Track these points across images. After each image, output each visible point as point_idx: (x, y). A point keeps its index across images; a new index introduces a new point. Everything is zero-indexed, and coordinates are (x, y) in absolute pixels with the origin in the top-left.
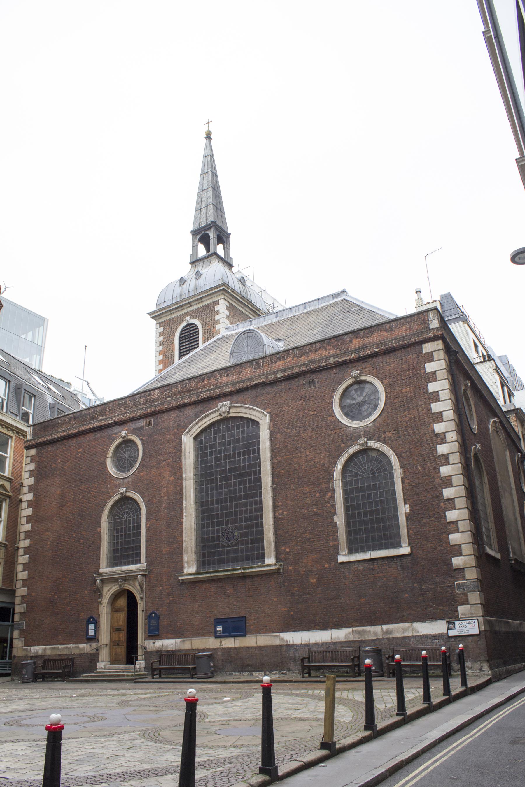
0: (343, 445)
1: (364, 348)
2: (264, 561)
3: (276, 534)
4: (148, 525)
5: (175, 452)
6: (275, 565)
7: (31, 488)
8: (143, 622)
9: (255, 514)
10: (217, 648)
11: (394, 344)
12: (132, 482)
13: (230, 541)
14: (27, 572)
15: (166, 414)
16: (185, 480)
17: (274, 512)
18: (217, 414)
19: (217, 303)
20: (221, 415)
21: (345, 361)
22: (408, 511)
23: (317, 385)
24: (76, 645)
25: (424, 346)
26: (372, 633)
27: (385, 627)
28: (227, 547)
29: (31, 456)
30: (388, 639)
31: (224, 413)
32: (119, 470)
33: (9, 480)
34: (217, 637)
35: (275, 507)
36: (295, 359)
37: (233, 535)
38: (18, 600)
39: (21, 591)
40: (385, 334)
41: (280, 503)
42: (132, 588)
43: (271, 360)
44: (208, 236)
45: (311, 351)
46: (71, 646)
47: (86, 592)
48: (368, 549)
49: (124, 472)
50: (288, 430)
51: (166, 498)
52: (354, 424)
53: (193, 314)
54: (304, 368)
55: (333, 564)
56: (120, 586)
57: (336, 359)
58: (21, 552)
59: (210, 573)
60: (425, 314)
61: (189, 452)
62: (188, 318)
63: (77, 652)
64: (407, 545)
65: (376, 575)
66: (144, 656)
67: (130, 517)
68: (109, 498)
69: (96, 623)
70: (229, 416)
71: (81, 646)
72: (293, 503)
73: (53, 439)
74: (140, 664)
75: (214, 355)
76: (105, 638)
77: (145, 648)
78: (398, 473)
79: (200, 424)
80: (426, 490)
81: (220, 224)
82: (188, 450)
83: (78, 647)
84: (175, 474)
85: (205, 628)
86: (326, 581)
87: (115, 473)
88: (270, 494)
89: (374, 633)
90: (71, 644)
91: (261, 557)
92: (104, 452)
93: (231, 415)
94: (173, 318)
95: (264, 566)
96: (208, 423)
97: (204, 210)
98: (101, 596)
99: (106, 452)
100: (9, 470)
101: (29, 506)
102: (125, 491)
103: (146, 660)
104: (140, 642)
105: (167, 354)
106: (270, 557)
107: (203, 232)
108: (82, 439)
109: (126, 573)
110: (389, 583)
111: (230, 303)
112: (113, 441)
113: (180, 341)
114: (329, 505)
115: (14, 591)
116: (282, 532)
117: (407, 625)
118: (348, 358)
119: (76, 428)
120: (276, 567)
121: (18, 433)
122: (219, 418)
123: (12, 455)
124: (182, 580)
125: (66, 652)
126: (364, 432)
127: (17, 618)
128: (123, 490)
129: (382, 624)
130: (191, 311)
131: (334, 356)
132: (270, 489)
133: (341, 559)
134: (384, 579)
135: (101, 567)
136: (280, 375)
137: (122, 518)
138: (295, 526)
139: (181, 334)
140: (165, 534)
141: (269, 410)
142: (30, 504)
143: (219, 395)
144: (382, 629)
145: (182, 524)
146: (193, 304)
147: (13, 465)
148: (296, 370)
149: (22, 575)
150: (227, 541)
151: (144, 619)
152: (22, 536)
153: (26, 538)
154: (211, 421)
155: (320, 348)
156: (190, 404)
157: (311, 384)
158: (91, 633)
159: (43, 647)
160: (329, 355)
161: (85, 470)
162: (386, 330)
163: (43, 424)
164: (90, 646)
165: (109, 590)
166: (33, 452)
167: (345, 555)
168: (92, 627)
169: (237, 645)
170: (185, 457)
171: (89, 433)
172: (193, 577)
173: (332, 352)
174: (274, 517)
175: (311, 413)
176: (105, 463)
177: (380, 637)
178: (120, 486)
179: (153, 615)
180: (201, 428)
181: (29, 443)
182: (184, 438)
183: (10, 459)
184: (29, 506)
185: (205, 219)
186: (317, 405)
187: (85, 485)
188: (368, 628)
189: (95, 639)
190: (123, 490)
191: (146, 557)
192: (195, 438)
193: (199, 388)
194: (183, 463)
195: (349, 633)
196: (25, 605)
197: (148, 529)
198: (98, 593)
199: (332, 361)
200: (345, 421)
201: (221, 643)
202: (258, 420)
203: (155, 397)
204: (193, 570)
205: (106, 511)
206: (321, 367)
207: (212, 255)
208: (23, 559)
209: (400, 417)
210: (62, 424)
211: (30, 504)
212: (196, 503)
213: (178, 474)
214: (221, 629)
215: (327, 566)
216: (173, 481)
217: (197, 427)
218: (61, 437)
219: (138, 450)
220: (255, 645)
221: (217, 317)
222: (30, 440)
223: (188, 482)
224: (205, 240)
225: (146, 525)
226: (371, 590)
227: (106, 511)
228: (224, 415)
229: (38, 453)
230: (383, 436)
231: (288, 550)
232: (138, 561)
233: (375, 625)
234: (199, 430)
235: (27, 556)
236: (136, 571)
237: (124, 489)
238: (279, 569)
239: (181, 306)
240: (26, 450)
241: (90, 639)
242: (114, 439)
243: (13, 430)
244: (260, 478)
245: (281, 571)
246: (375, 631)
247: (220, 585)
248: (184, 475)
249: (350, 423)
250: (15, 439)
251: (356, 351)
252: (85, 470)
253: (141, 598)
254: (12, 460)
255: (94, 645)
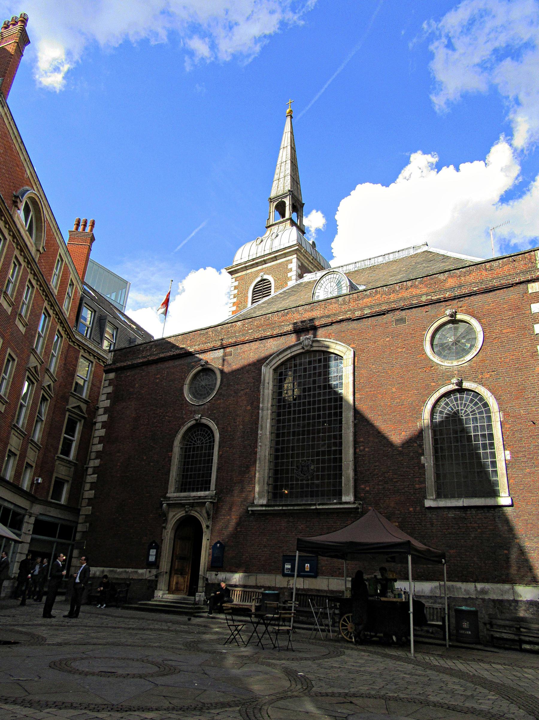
0: (433, 384)
1: (460, 287)
2: (341, 498)
3: (355, 471)
4: (221, 453)
5: (254, 383)
6: (354, 503)
7: (107, 410)
8: (207, 551)
9: (333, 448)
10: (284, 588)
11: (496, 283)
12: (208, 409)
13: (305, 475)
14: (94, 491)
15: (247, 345)
16: (262, 410)
17: (355, 448)
18: (300, 347)
19: (291, 262)
20: (303, 348)
21: (439, 299)
22: (508, 457)
23: (407, 323)
24: (135, 570)
25: (530, 285)
26: (463, 590)
27: (479, 586)
28: (302, 480)
29: (109, 380)
30: (483, 600)
31: (307, 346)
32: (195, 397)
33: (86, 402)
34: (285, 575)
35: (356, 442)
36: (383, 296)
37: (308, 469)
38: (81, 519)
39: (86, 510)
40: (484, 273)
41: (361, 439)
42: (199, 515)
43: (358, 297)
44: (284, 203)
45: (402, 288)
46: (130, 570)
47: (151, 515)
48: (460, 496)
49: (199, 399)
50: (374, 366)
51: (241, 427)
52: (446, 364)
53: (268, 271)
54: (393, 306)
55: (418, 509)
56: (186, 512)
57: (429, 297)
58: (90, 471)
59: (283, 506)
60: (532, 253)
61: (268, 383)
62: (262, 274)
63: (135, 577)
64: (507, 494)
65: (469, 525)
66: (204, 588)
67: (203, 443)
68: (183, 424)
69: (158, 548)
70: (312, 349)
71: (140, 571)
72: (376, 440)
73: (133, 365)
74: (200, 596)
75: (292, 298)
76: (165, 565)
77: (207, 579)
78: (496, 417)
79: (281, 357)
80: (531, 436)
81: (296, 194)
82: (267, 381)
83: (137, 572)
84: (252, 404)
85: (273, 564)
86: (410, 526)
87: (191, 400)
88: (352, 429)
89: (465, 590)
90: (130, 568)
91: (339, 494)
92: (182, 379)
93: (314, 349)
94: (248, 273)
95: (341, 503)
96: (289, 356)
97: (282, 180)
98: (166, 521)
99: (184, 379)
100: (87, 393)
101: (103, 427)
102: (200, 418)
103: (207, 593)
104: (201, 573)
105: (240, 306)
106: (348, 495)
107: (280, 200)
108: (161, 366)
109: (194, 500)
110: (484, 535)
111: (302, 263)
112: (192, 368)
113: (253, 294)
114: (415, 445)
115: (79, 510)
116: (362, 469)
117: (507, 586)
118: (442, 296)
119: (156, 355)
120: (355, 506)
121: (99, 359)
122: (301, 351)
123: (91, 379)
124: (252, 511)
125: (124, 576)
126: (458, 371)
127: (78, 537)
128: (198, 416)
129: (475, 581)
130: (265, 268)
131: (427, 295)
132: (351, 424)
133: (428, 503)
134: (479, 530)
135: (169, 491)
136: (367, 311)
137: (194, 444)
138: (377, 464)
139: (254, 289)
140: (237, 463)
141: (354, 346)
142: (104, 425)
143: (303, 328)
144: (475, 587)
145: (256, 453)
146: (268, 261)
147: (91, 389)
148: (384, 308)
149: (89, 494)
150: (302, 475)
151: (208, 548)
152: (93, 455)
153: (96, 458)
154: (293, 354)
155: (411, 286)
156: (272, 337)
157: (402, 320)
158: (152, 558)
159: (101, 569)
160: (422, 292)
161: (161, 396)
162: (486, 269)
163: (124, 351)
164: (150, 572)
165: (174, 516)
166: (112, 375)
167: (434, 500)
168: (153, 552)
169: (306, 587)
170: (264, 388)
171: (169, 360)
172: (264, 508)
173: (424, 290)
174: (355, 453)
175: (400, 350)
176: (182, 390)
177: (474, 597)
178: (195, 412)
179: (218, 545)
180: (282, 360)
181: (109, 367)
182: (263, 368)
183: (89, 383)
184: (103, 427)
185: (282, 188)
186: (406, 342)
187: (160, 409)
188: (459, 584)
189: (156, 565)
190: (198, 416)
191: (216, 485)
192: (275, 370)
193: (283, 322)
194: (261, 393)
195: (435, 587)
196: (88, 524)
197: (220, 457)
198: (163, 517)
199: (424, 299)
200: (436, 359)
201: (288, 582)
202: (342, 355)
203: (237, 328)
204: (264, 501)
205: (179, 436)
206: (412, 304)
207: (287, 220)
208: (92, 478)
209: (500, 358)
210: (143, 351)
211: (104, 425)
212: (271, 433)
213: (255, 403)
214: (289, 567)
215: (411, 509)
216: (249, 410)
217: (278, 359)
218: (141, 363)
219: (216, 379)
220: (326, 589)
221: (289, 275)
222: (110, 365)
223: (265, 412)
224: (281, 208)
225: (219, 452)
226: (462, 541)
227: (179, 436)
228: (306, 349)
229: (116, 377)
230: (480, 376)
231: (368, 488)
232: (208, 489)
233: (467, 582)
234: (279, 362)
235: (96, 475)
236: (205, 497)
237: (200, 415)
238: (357, 508)
239: (257, 263)
240: (106, 373)
241: (150, 565)
242: (193, 367)
243: (94, 356)
244: (341, 413)
245: (360, 510)
246: (467, 589)
247: (291, 519)
248: (261, 405)
249: (442, 362)
250: (96, 365)
251: (452, 289)
252: (161, 396)
253: (208, 527)
254: (90, 384)
255: (154, 572)
